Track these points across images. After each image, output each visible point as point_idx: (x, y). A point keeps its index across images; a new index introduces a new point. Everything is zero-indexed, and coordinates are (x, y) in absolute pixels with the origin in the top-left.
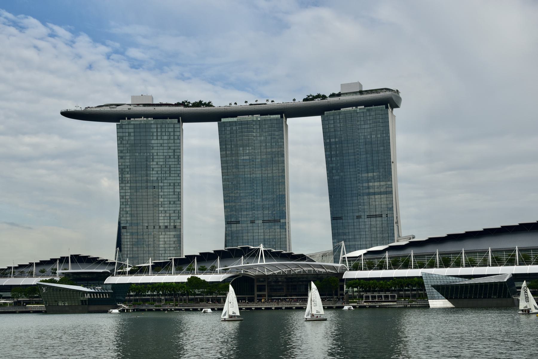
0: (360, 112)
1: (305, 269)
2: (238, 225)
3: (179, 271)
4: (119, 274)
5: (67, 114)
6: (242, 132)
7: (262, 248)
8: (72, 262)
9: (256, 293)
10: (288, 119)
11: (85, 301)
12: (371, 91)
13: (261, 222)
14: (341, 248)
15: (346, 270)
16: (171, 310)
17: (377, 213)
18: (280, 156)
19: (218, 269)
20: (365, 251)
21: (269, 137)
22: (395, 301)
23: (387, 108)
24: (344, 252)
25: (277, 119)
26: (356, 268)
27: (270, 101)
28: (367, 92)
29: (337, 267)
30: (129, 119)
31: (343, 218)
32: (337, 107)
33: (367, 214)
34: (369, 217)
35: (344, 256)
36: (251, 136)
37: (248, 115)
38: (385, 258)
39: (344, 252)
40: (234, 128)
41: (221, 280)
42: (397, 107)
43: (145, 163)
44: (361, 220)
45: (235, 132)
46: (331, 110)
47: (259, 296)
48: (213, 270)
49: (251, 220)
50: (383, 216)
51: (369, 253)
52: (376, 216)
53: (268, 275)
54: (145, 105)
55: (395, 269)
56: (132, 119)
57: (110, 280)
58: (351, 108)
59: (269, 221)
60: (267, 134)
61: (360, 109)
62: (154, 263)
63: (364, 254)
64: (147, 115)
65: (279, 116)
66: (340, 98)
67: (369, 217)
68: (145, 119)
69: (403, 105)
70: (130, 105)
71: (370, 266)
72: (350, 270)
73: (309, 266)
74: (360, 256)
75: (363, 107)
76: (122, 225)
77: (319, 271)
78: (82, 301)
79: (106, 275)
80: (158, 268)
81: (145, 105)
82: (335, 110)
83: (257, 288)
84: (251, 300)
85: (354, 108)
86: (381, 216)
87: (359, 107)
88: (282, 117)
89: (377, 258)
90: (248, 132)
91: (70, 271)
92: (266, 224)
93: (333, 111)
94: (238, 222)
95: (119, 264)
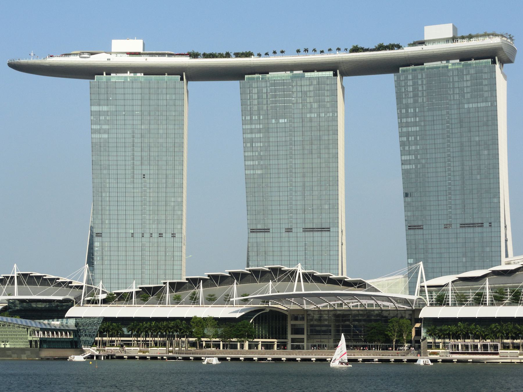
0: (452, 70)
1: (364, 302)
2: (266, 234)
3: (177, 301)
4: (89, 302)
6: (275, 96)
7: (300, 270)
8: (20, 283)
9: (290, 336)
10: (345, 78)
11: (36, 342)
13: (302, 230)
14: (417, 273)
15: (424, 305)
16: (162, 358)
17: (476, 221)
18: (331, 132)
19: (235, 299)
20: (454, 277)
21: (315, 105)
22: (497, 354)
23: (494, 62)
24: (422, 278)
25: (328, 78)
26: (441, 301)
29: (412, 301)
31: (424, 227)
32: (418, 61)
33: (460, 221)
34: (463, 226)
35: (422, 284)
37: (285, 70)
38: (483, 288)
39: (422, 278)
41: (237, 315)
42: (510, 61)
43: (131, 140)
44: (450, 231)
45: (265, 96)
46: (409, 65)
47: (293, 340)
48: (226, 300)
49: (287, 227)
50: (485, 225)
51: (461, 279)
52: (473, 225)
53: (307, 311)
55: (499, 305)
56: (112, 75)
57: (73, 312)
58: (440, 62)
59: (312, 230)
60: (312, 100)
61: (453, 64)
62: (140, 288)
63: (453, 282)
64: (135, 70)
65: (331, 73)
66: (424, 46)
67: (463, 226)
68: (132, 75)
69: (518, 58)
71: (461, 301)
72: (431, 305)
73: (370, 297)
74: (447, 285)
75: (458, 61)
76: (95, 231)
77: (384, 306)
78: (31, 342)
79: (67, 304)
80: (147, 294)
82: (416, 65)
83: (292, 329)
84: (282, 346)
85: (444, 62)
86: (481, 225)
87: (451, 62)
88: (335, 75)
89: (473, 289)
90: (284, 96)
91: (16, 297)
92: (307, 234)
94: (266, 231)
95: (89, 289)
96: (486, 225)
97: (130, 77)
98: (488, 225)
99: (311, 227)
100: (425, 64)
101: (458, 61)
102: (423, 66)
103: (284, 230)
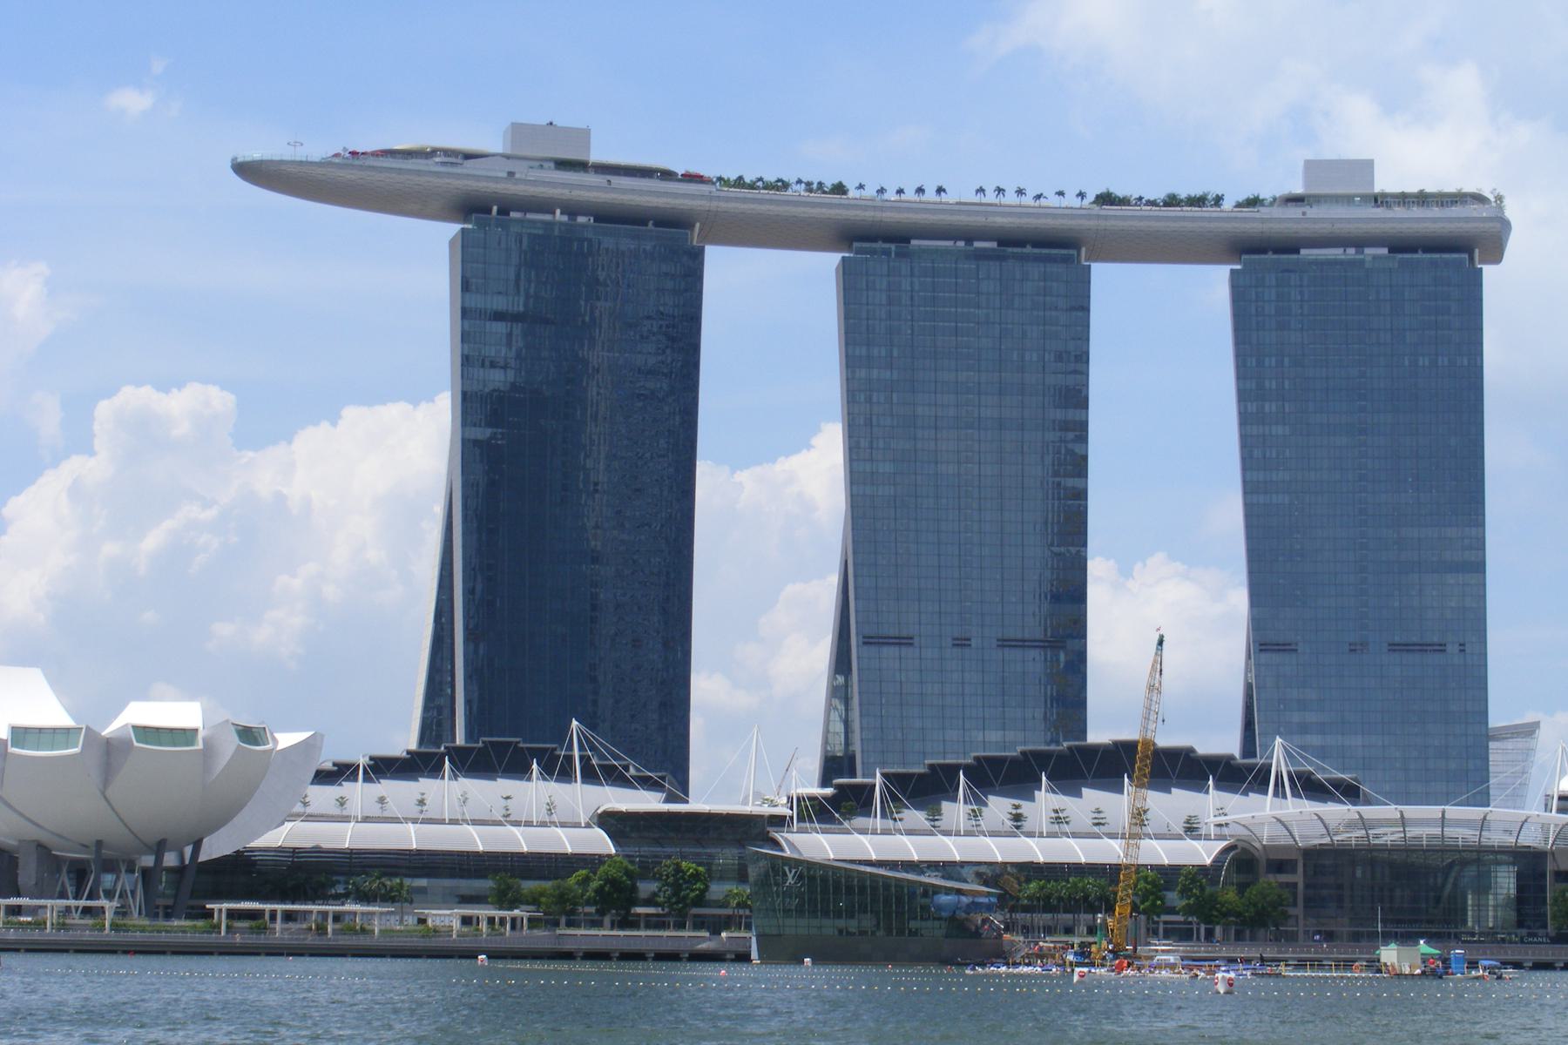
2: (905, 651)
5: (249, 171)
12: (1422, 199)
23: (1472, 259)
27: (1031, 193)
28: (1403, 199)
30: (504, 211)
36: (970, 320)
37: (955, 238)
40: (906, 285)
50: (1449, 648)
54: (562, 164)
58: (1341, 251)
66: (1307, 209)
68: (565, 218)
70: (508, 157)
75: (1385, 251)
81: (562, 164)
82: (1277, 251)
85: (1351, 251)
87: (1369, 251)
92: (1011, 654)
93: (1270, 256)
94: (904, 641)
96: (1452, 649)
97: (561, 223)
98: (1457, 648)
99: (1019, 636)
100: (1303, 252)
101: (1385, 251)
102: (1295, 256)
103: (950, 642)
